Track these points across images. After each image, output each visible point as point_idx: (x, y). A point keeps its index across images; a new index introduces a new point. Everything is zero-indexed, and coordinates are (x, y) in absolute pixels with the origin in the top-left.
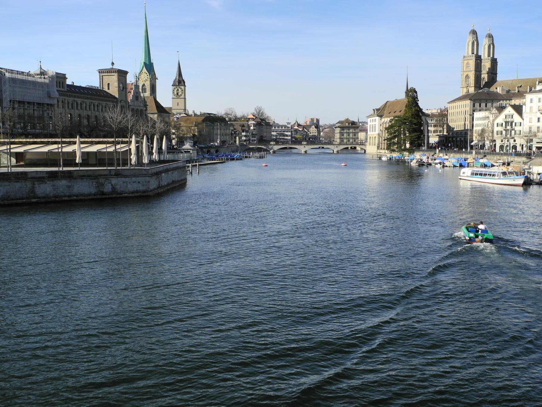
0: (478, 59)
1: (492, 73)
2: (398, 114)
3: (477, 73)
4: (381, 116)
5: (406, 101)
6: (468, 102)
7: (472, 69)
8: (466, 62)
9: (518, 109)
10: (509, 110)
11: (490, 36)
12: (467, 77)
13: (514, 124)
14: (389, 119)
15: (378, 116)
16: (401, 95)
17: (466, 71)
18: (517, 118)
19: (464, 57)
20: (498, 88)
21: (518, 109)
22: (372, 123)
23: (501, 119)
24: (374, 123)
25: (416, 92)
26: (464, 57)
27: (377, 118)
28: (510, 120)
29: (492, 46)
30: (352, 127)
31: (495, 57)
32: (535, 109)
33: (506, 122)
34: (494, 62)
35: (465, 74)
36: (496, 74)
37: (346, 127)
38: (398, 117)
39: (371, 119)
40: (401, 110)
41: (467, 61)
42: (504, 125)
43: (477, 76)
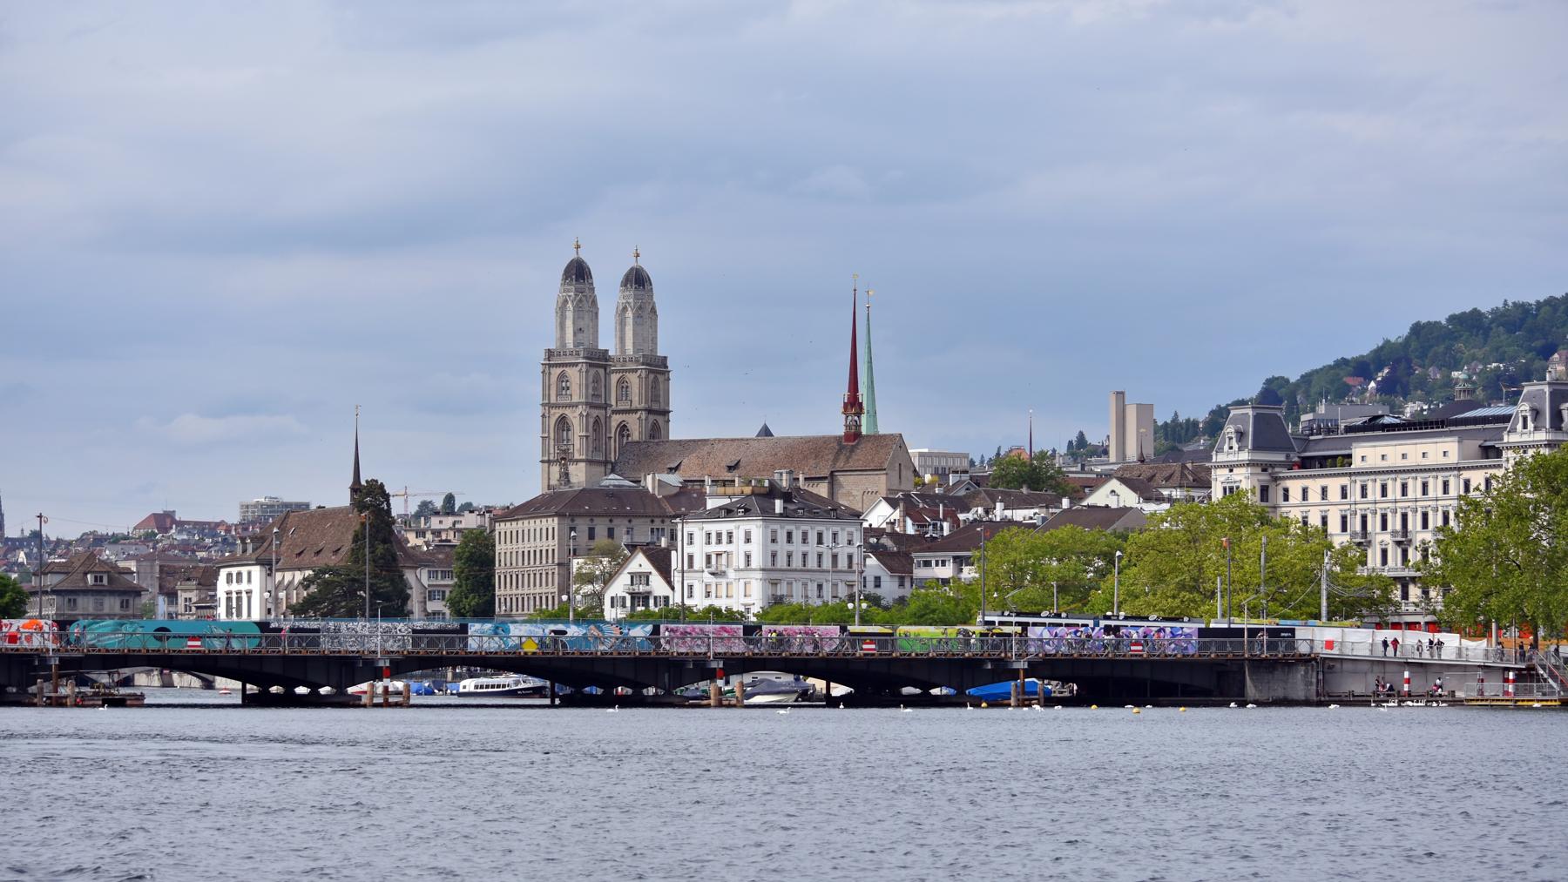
0: (598, 361)
1: (649, 411)
2: (333, 560)
3: (595, 412)
4: (268, 565)
5: (356, 520)
6: (553, 523)
7: (575, 399)
8: (556, 371)
9: (662, 562)
10: (640, 563)
11: (638, 280)
12: (563, 423)
13: (652, 602)
14: (299, 576)
15: (259, 562)
16: (341, 498)
17: (558, 406)
18: (658, 586)
19: (550, 353)
20: (649, 478)
21: (662, 562)
22: (235, 587)
23: (620, 586)
24: (244, 586)
25: (387, 497)
26: (550, 353)
27: (256, 571)
28: (642, 588)
29: (645, 313)
30: (112, 593)
31: (660, 353)
32: (699, 562)
33: (634, 596)
34: (657, 369)
35: (557, 413)
36: (666, 413)
37: (86, 592)
38: (334, 571)
39: (234, 570)
40: (337, 550)
41: (559, 370)
42: (628, 603)
43: (597, 422)
